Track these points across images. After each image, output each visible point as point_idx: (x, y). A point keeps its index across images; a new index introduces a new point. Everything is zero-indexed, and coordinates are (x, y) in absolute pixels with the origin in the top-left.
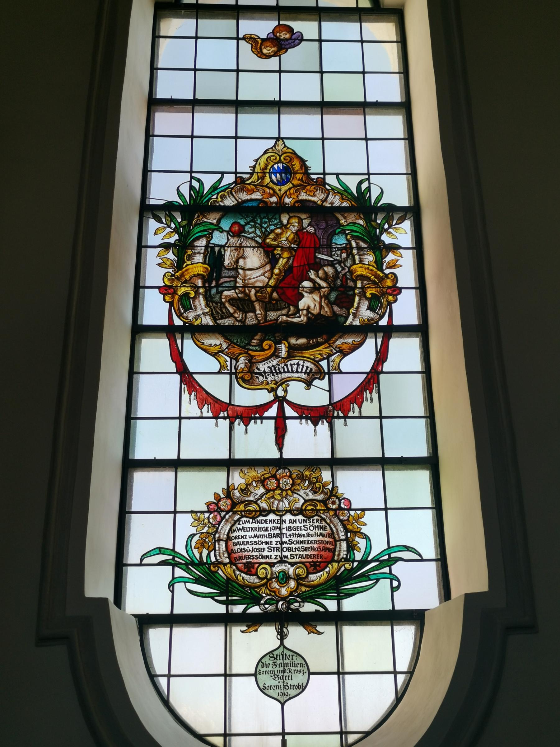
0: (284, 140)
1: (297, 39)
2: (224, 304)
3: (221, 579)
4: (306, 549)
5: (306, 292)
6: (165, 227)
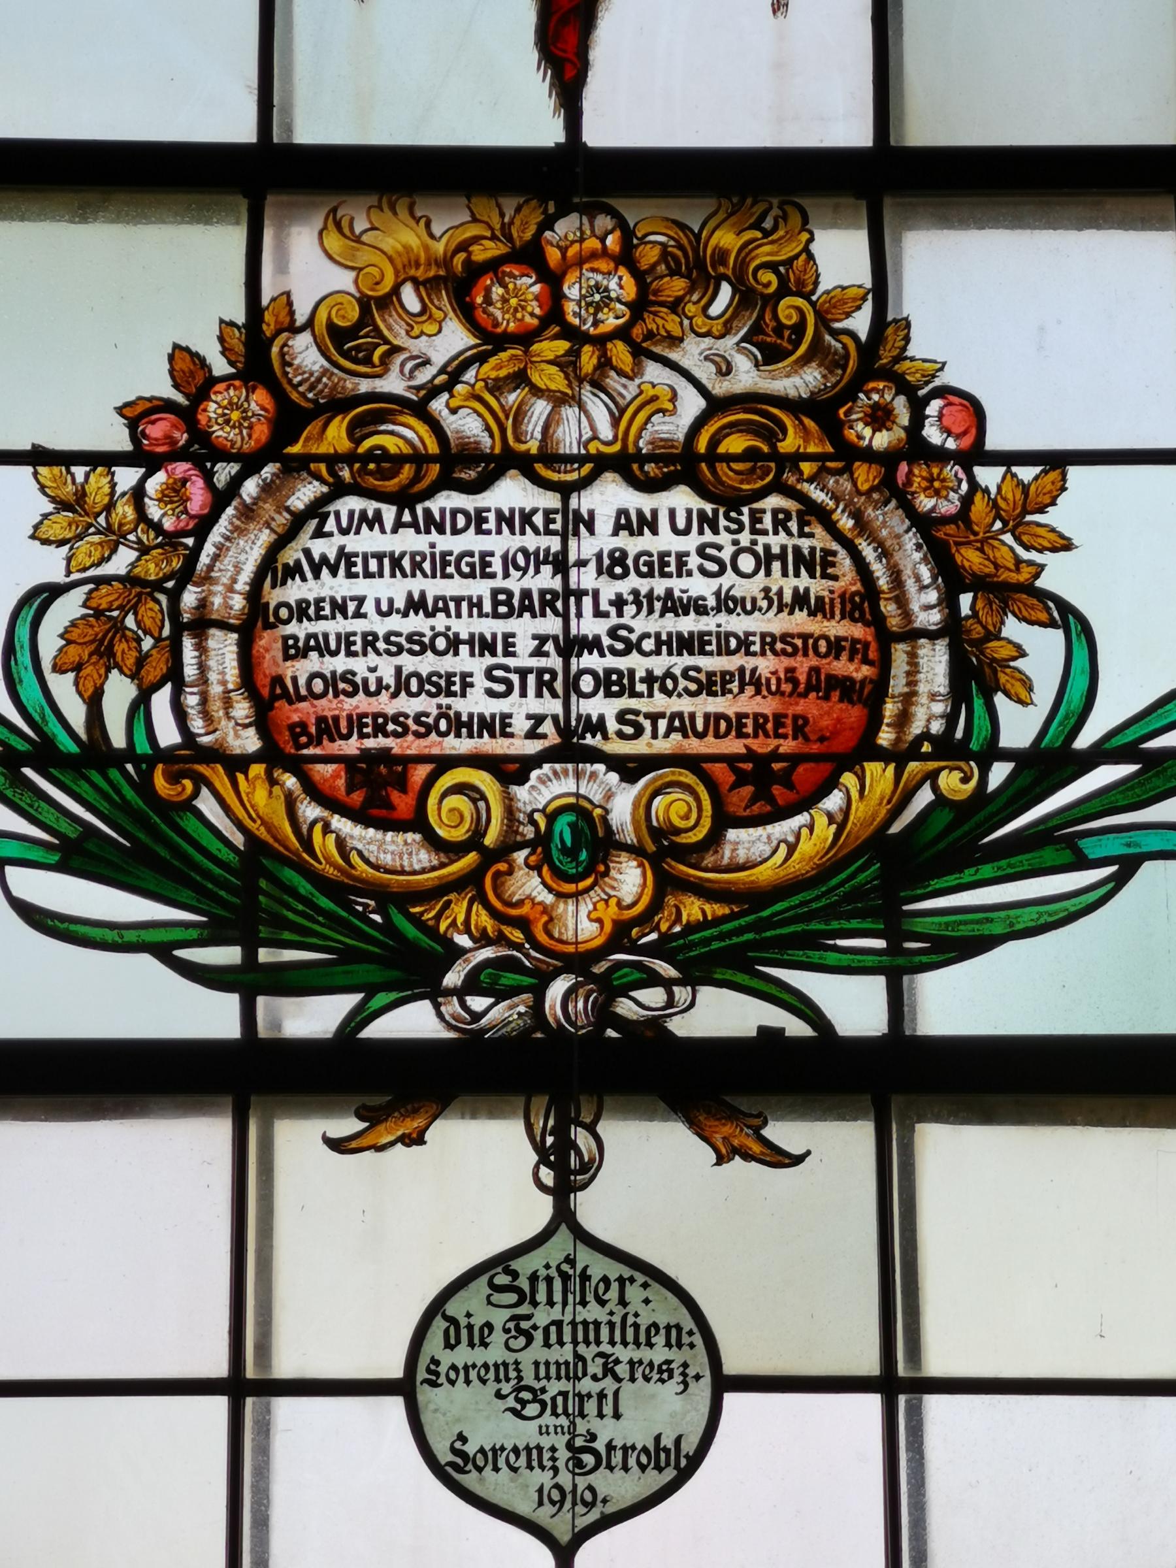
3: (214, 846)
4: (710, 685)
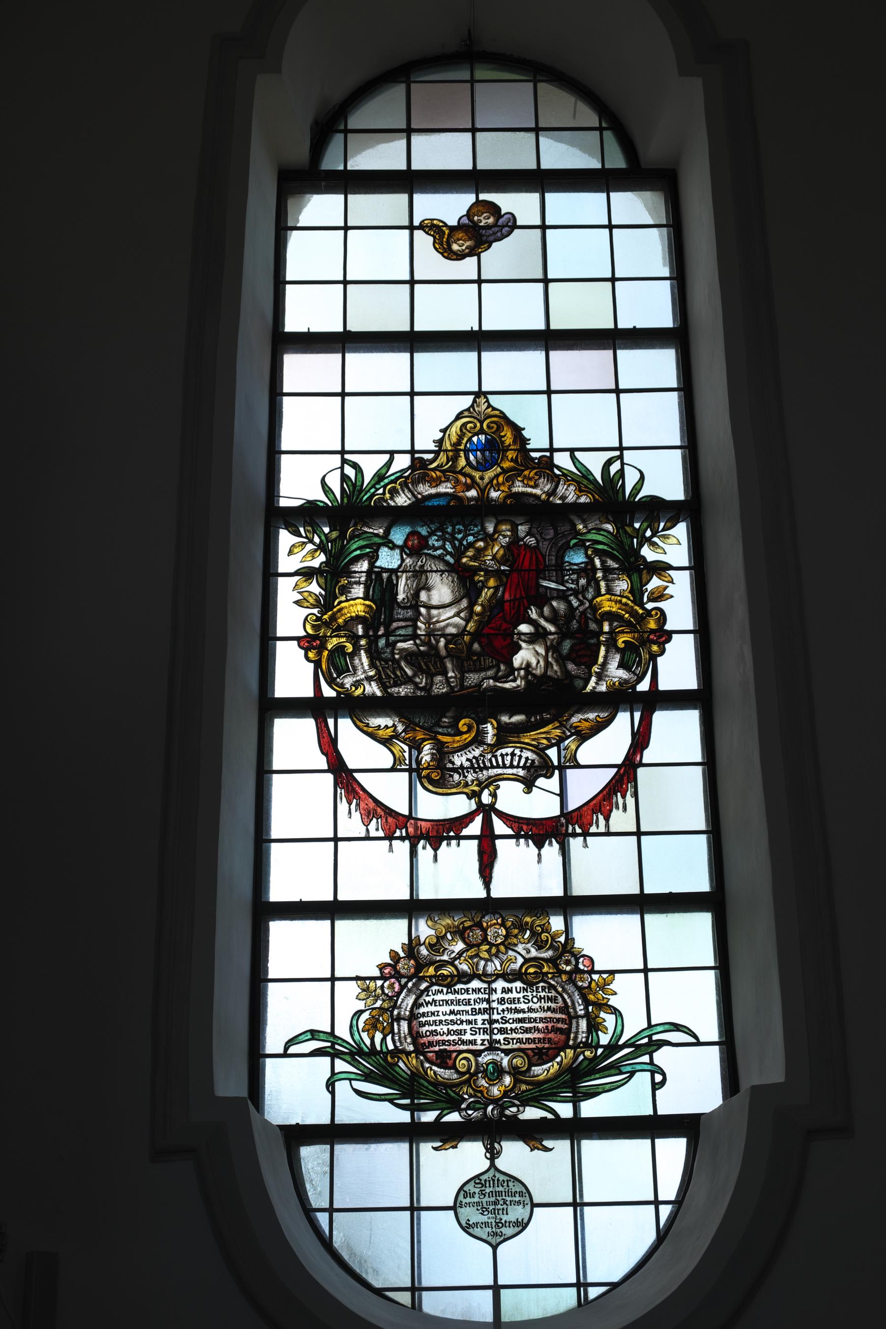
0: (489, 396)
1: (507, 226)
2: (398, 662)
3: (403, 1074)
4: (528, 1030)
5: (524, 641)
6: (304, 543)
